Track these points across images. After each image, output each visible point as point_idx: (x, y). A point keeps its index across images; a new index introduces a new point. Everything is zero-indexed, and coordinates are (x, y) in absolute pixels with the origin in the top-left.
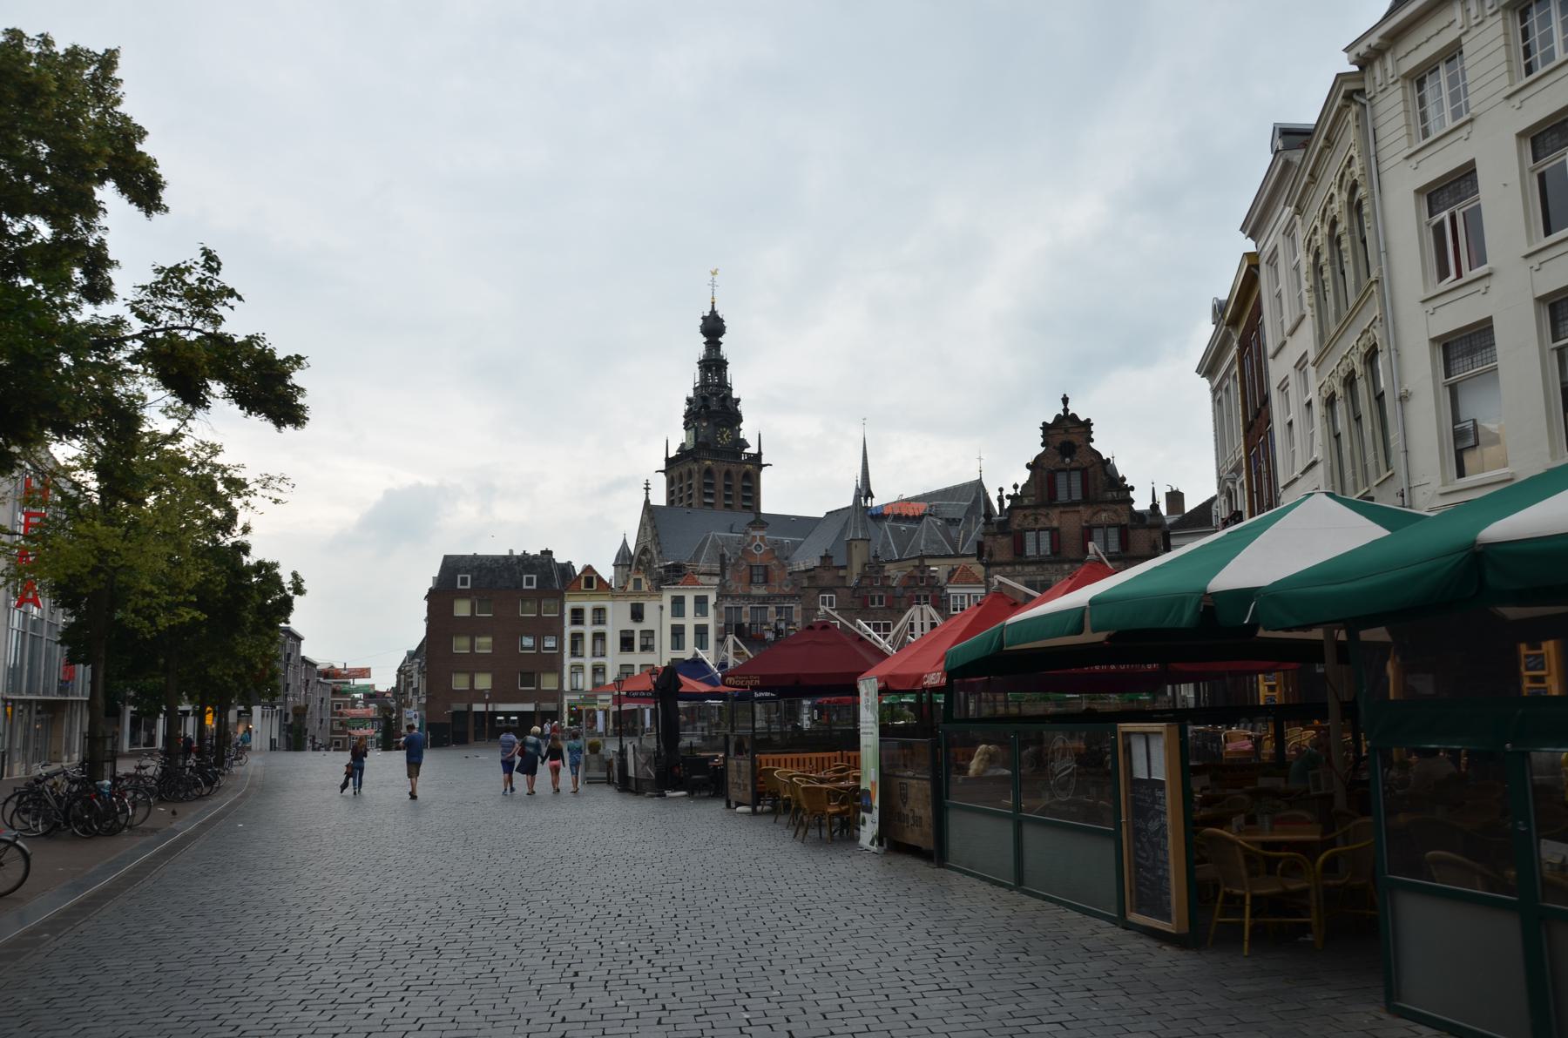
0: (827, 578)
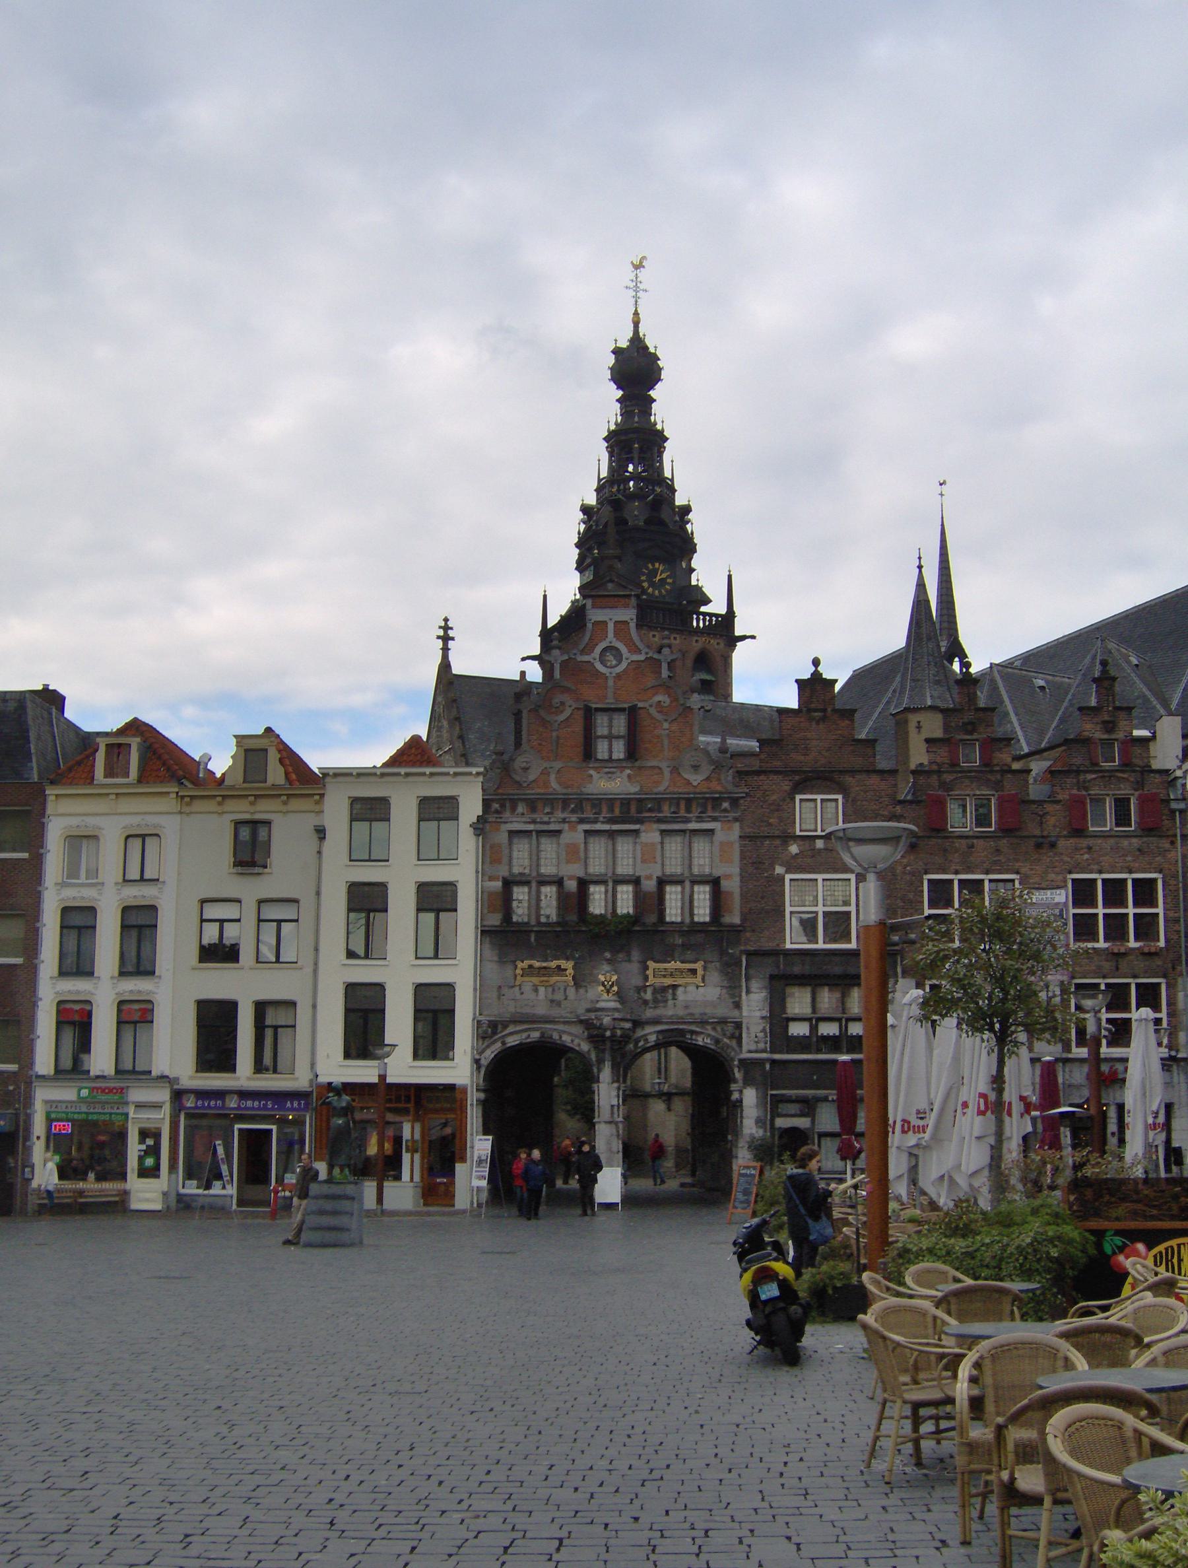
0: (818, 746)
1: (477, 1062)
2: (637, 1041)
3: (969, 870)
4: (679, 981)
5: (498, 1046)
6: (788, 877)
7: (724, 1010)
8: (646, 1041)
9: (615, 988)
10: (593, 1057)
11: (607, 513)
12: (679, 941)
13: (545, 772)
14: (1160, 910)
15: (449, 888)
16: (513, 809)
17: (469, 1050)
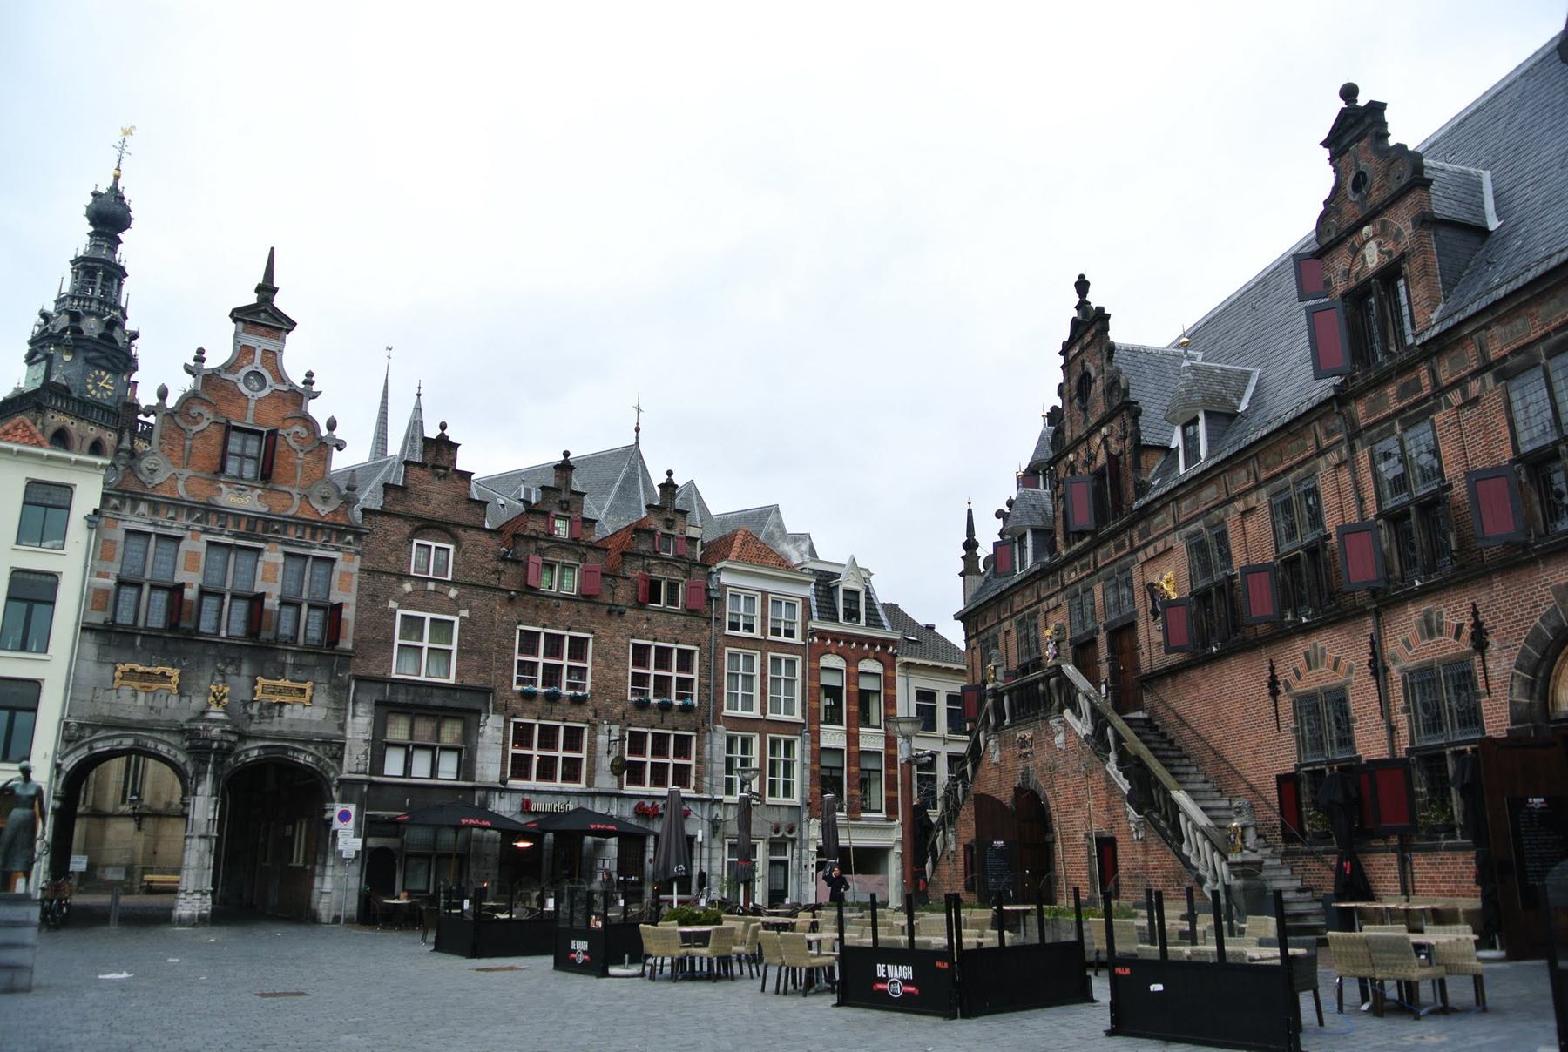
1: (58, 767)
2: (239, 754)
3: (554, 626)
4: (287, 699)
5: (82, 753)
6: (400, 612)
7: (330, 730)
8: (247, 756)
9: (226, 700)
10: (190, 769)
11: (64, 321)
12: (290, 660)
13: (174, 478)
14: (695, 676)
15: (49, 579)
16: (134, 509)
17: (50, 753)
